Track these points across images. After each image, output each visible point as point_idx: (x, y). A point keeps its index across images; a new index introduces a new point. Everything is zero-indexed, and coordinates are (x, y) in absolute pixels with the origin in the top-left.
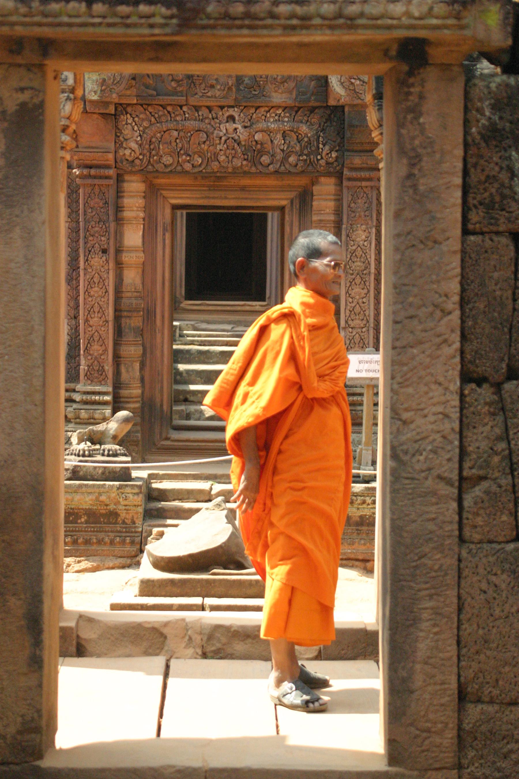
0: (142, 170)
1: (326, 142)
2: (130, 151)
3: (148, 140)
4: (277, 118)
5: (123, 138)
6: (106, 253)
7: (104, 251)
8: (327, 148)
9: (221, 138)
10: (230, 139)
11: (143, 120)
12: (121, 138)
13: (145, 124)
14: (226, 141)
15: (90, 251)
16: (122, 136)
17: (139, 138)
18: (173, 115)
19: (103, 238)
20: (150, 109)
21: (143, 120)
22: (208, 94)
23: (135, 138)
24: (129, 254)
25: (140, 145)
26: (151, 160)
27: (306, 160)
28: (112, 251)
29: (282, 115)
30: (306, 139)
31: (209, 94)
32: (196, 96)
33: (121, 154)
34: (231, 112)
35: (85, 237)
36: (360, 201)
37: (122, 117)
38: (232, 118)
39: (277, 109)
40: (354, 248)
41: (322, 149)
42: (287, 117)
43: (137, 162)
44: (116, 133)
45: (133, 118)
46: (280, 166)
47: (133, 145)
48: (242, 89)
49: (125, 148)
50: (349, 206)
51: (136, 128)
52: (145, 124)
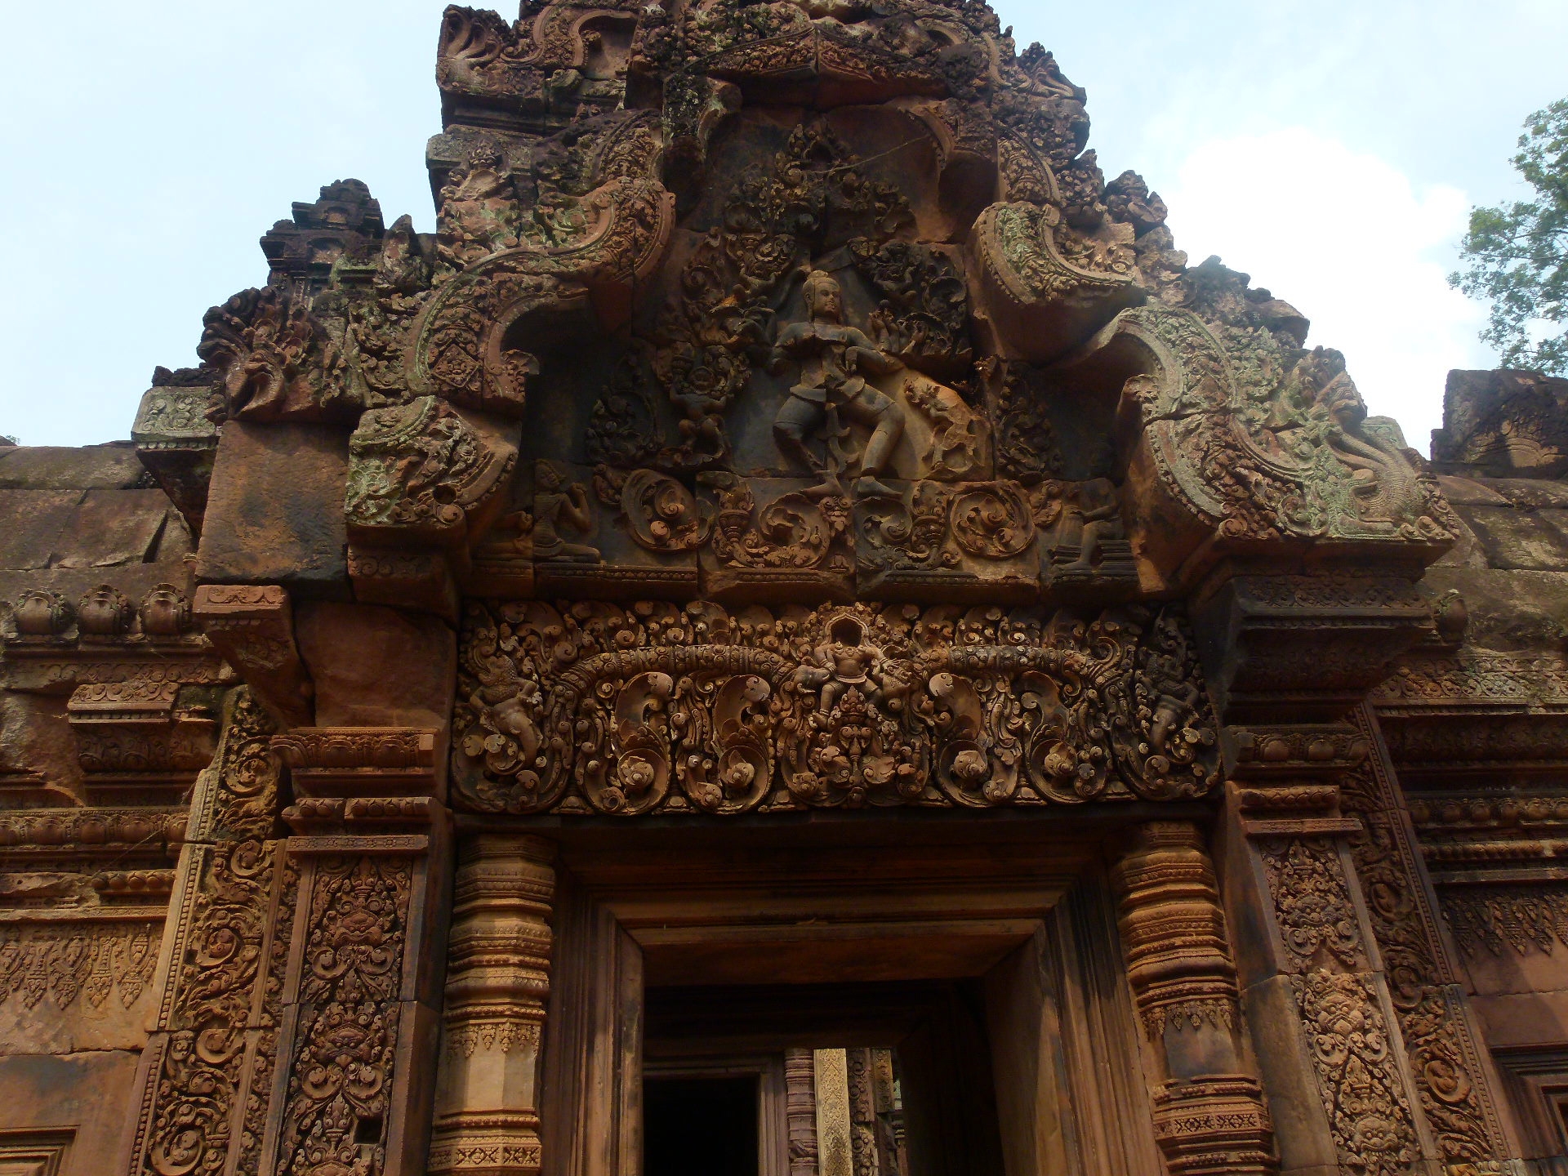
0: (545, 813)
1: (1158, 699)
2: (502, 740)
3: (570, 707)
4: (988, 632)
5: (483, 698)
6: (374, 1138)
7: (370, 1129)
8: (1164, 715)
9: (817, 686)
10: (852, 691)
11: (552, 640)
12: (475, 700)
13: (563, 649)
14: (836, 698)
15: (305, 1133)
16: (478, 692)
17: (536, 698)
18: (654, 626)
19: (367, 1073)
20: (577, 609)
21: (552, 640)
22: (768, 557)
23: (521, 695)
24: (478, 1143)
25: (540, 722)
26: (579, 770)
27: (1103, 758)
28: (397, 1128)
29: (1005, 624)
30: (1092, 693)
31: (773, 557)
32: (733, 563)
33: (471, 752)
34: (843, 613)
35: (293, 1071)
36: (1308, 886)
37: (483, 632)
38: (847, 633)
39: (988, 609)
40: (1337, 1058)
41: (1150, 720)
42: (1020, 630)
43: (528, 776)
44: (458, 687)
45: (521, 640)
46: (1018, 787)
47: (517, 718)
48: (877, 542)
49: (489, 733)
50: (1278, 908)
51: (527, 666)
52: (563, 649)
